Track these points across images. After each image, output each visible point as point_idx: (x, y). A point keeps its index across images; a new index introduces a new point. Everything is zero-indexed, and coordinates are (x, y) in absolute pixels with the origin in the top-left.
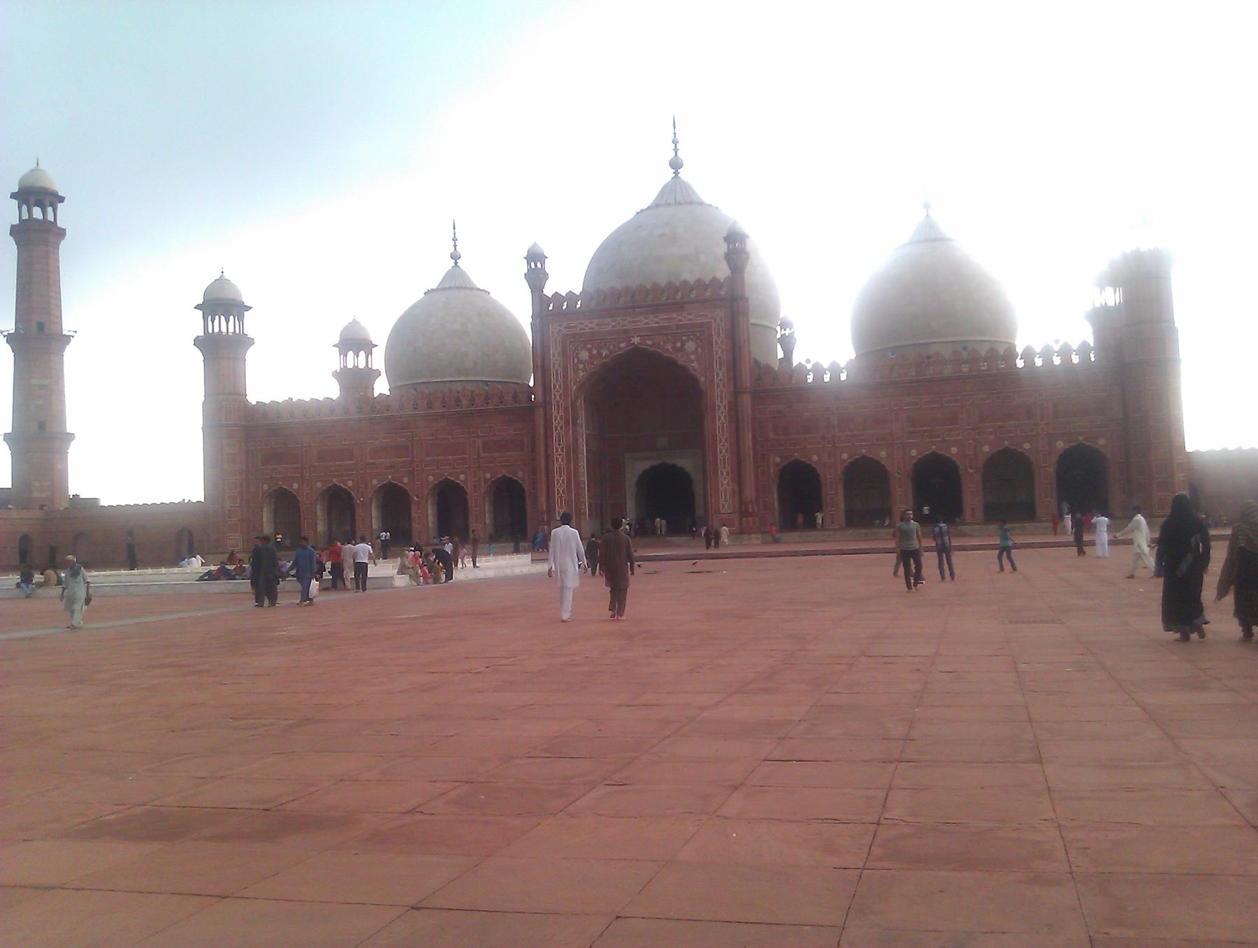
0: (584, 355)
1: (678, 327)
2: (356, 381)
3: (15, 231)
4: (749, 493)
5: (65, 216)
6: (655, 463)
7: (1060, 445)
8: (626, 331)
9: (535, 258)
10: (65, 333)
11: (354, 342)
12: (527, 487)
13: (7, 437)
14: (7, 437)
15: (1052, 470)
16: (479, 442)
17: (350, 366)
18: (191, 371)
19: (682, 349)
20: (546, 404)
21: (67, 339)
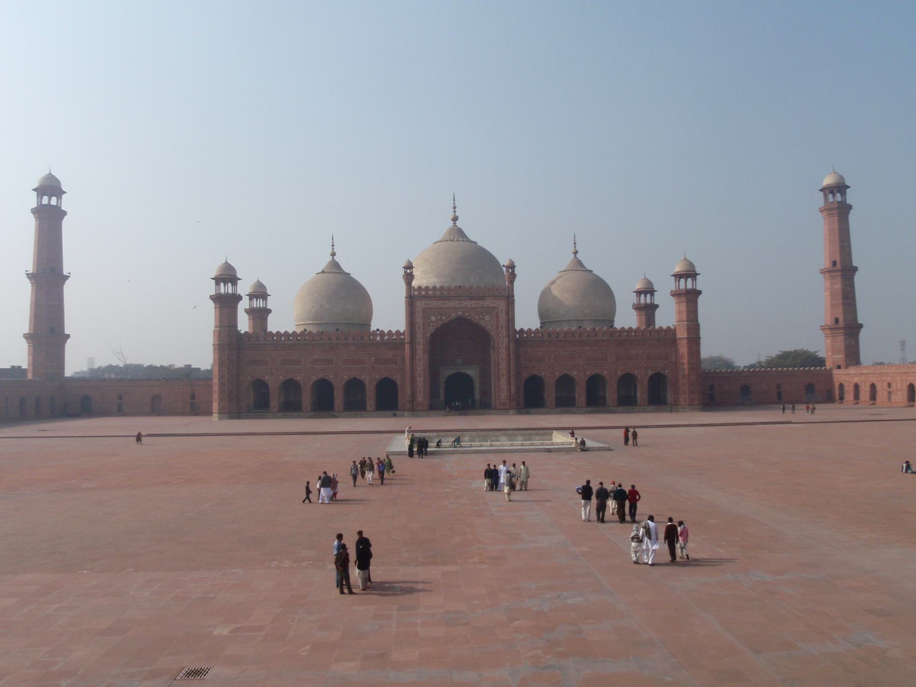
0: (433, 319)
1: (482, 308)
3: (35, 211)
4: (513, 390)
6: (455, 371)
7: (650, 372)
8: (456, 308)
9: (409, 266)
10: (65, 273)
12: (399, 383)
13: (27, 337)
14: (27, 337)
15: (646, 383)
16: (373, 359)
19: (483, 319)
20: (412, 342)
21: (67, 277)
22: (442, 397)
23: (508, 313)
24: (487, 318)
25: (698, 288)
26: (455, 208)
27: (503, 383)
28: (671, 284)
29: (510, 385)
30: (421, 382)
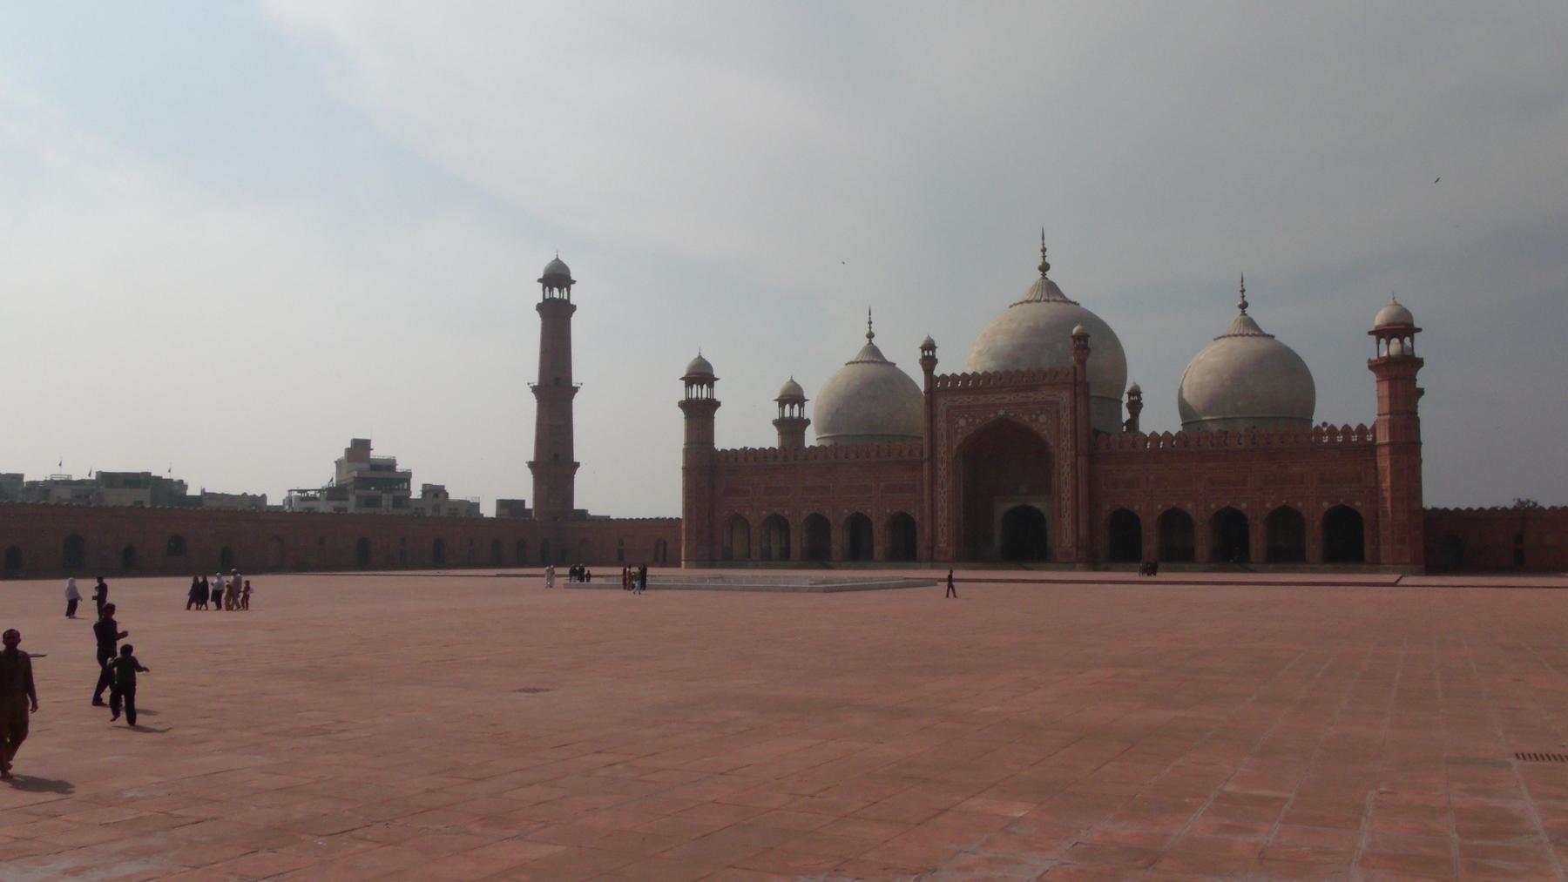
0: (962, 422)
2: (791, 428)
5: (576, 295)
7: (1326, 504)
9: (929, 346)
11: (793, 396)
12: (917, 519)
13: (531, 465)
14: (531, 465)
15: (1318, 523)
17: (787, 414)
18: (677, 423)
20: (933, 458)
21: (576, 390)
22: (997, 540)
23: (1074, 410)
24: (1042, 418)
25: (1418, 354)
26: (1044, 250)
27: (1067, 521)
28: (1372, 349)
29: (1077, 524)
30: (942, 518)
